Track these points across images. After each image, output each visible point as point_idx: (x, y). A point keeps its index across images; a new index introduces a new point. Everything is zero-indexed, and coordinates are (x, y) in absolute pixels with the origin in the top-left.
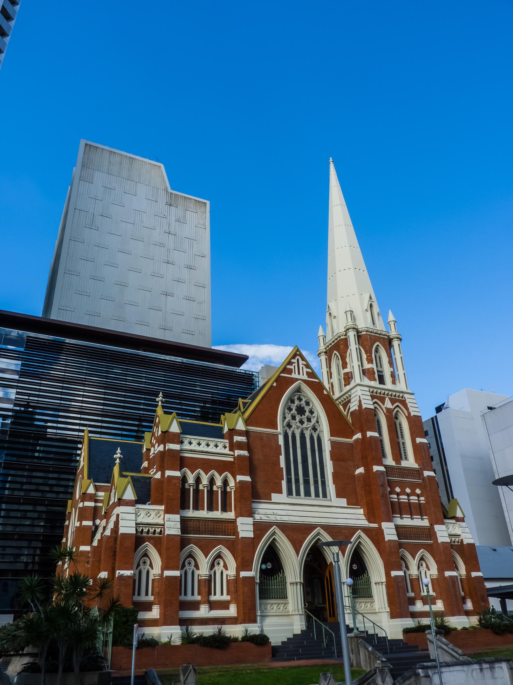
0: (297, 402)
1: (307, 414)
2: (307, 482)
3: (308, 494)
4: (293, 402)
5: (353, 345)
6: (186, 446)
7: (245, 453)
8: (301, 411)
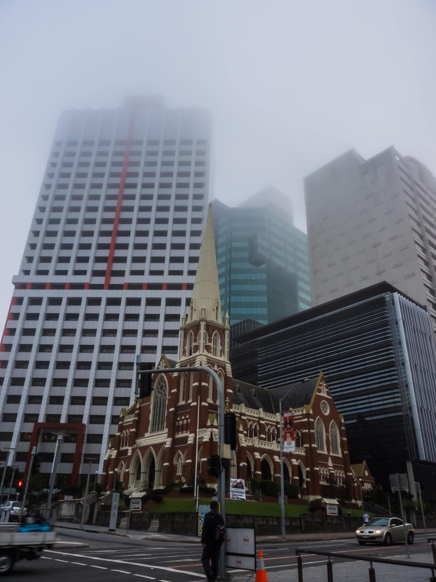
0: (161, 383)
1: (164, 388)
2: (159, 424)
3: (158, 430)
4: (160, 384)
5: (202, 331)
6: (126, 421)
7: (136, 418)
8: (162, 388)
